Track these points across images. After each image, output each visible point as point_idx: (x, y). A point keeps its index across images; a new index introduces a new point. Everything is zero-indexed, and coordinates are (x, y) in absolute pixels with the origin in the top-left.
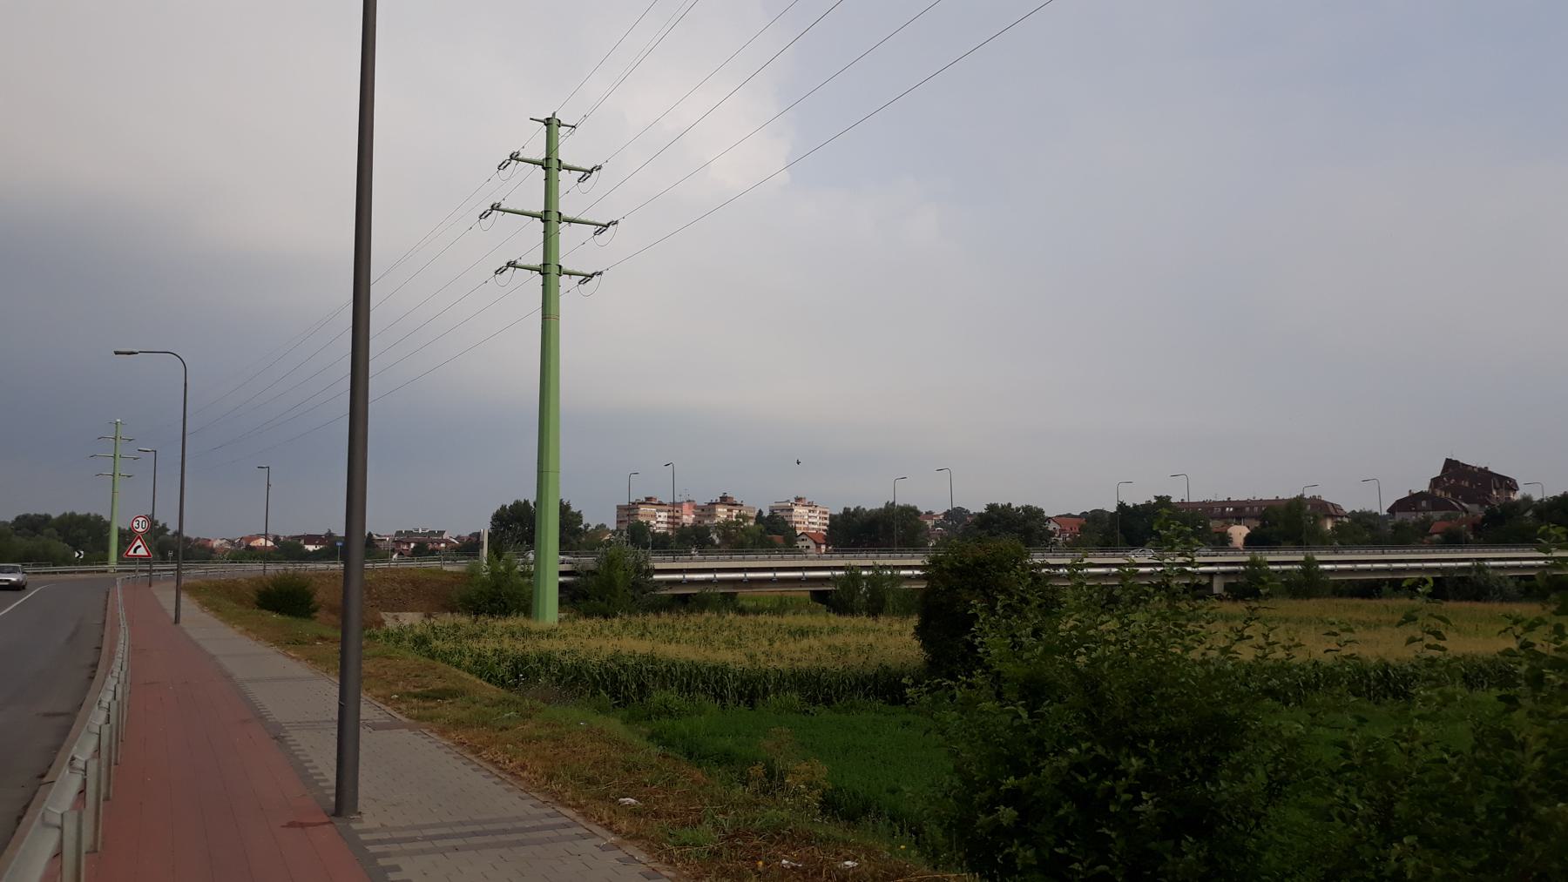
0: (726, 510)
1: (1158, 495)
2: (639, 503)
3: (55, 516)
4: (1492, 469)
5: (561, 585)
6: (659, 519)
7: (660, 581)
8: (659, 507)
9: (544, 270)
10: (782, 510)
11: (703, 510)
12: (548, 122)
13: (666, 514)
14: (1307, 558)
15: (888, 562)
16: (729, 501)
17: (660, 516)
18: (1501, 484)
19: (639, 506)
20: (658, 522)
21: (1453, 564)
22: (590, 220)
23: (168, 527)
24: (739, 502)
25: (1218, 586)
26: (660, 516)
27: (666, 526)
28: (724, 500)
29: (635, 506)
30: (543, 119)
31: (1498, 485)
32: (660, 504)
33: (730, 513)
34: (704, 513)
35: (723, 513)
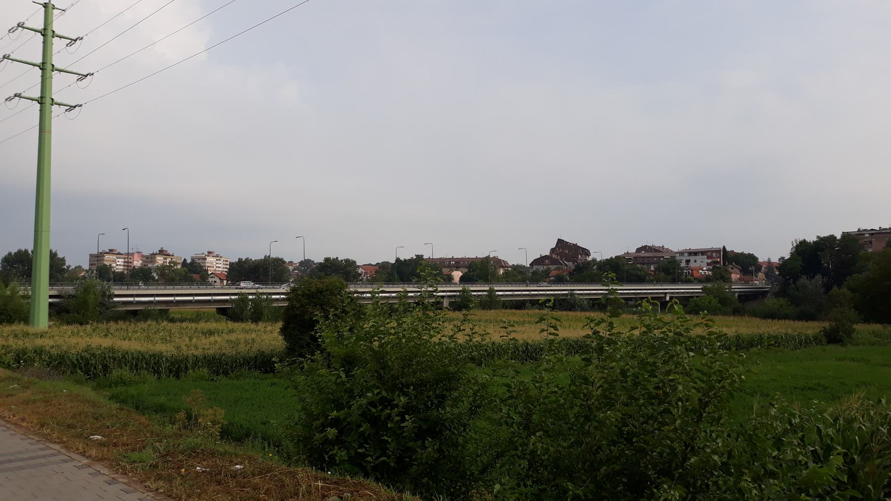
2: (104, 253)
5: (50, 304)
6: (118, 263)
7: (118, 302)
8: (118, 256)
9: (41, 101)
10: (199, 259)
11: (147, 258)
12: (45, 6)
13: (123, 260)
14: (490, 289)
16: (164, 253)
17: (119, 261)
18: (583, 252)
19: (105, 255)
20: (117, 265)
21: (560, 292)
22: (75, 71)
25: (446, 303)
26: (119, 261)
27: (123, 267)
28: (162, 252)
30: (42, 2)
31: (581, 253)
32: (119, 254)
33: (165, 260)
34: (148, 260)
35: (160, 260)
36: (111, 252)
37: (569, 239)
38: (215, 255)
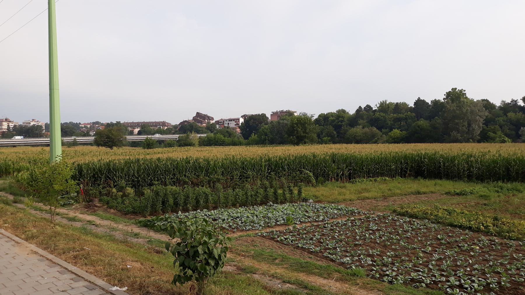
4: (209, 115)
10: (27, 123)
16: (8, 120)
28: (6, 120)
35: (5, 124)
37: (203, 112)
38: (36, 121)
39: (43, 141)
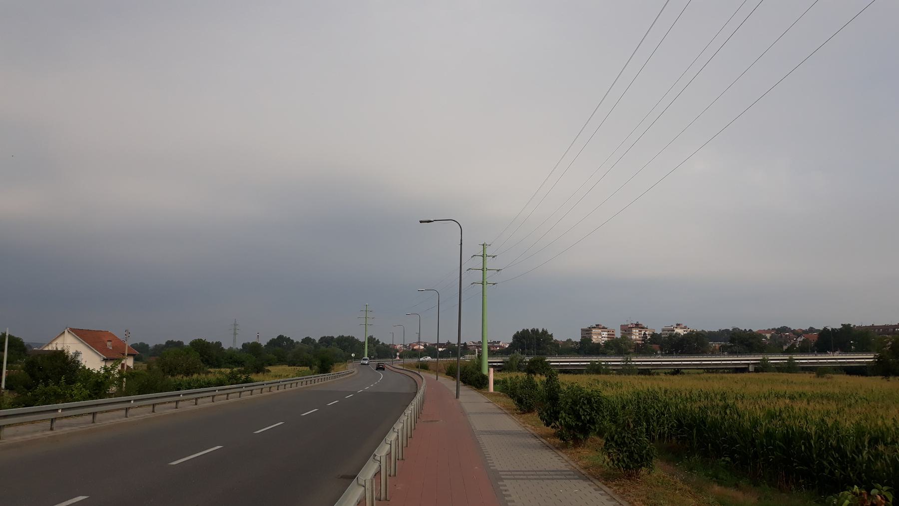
0: (638, 331)
1: (844, 324)
2: (592, 328)
3: (336, 337)
5: (489, 365)
6: (603, 336)
12: (483, 245)
13: (607, 333)
15: (603, 360)
23: (380, 340)
24: (646, 327)
25: (751, 368)
27: (607, 339)
28: (637, 326)
29: (590, 329)
33: (640, 333)
34: (626, 333)
36: (598, 326)
38: (683, 327)
39: (730, 362)
